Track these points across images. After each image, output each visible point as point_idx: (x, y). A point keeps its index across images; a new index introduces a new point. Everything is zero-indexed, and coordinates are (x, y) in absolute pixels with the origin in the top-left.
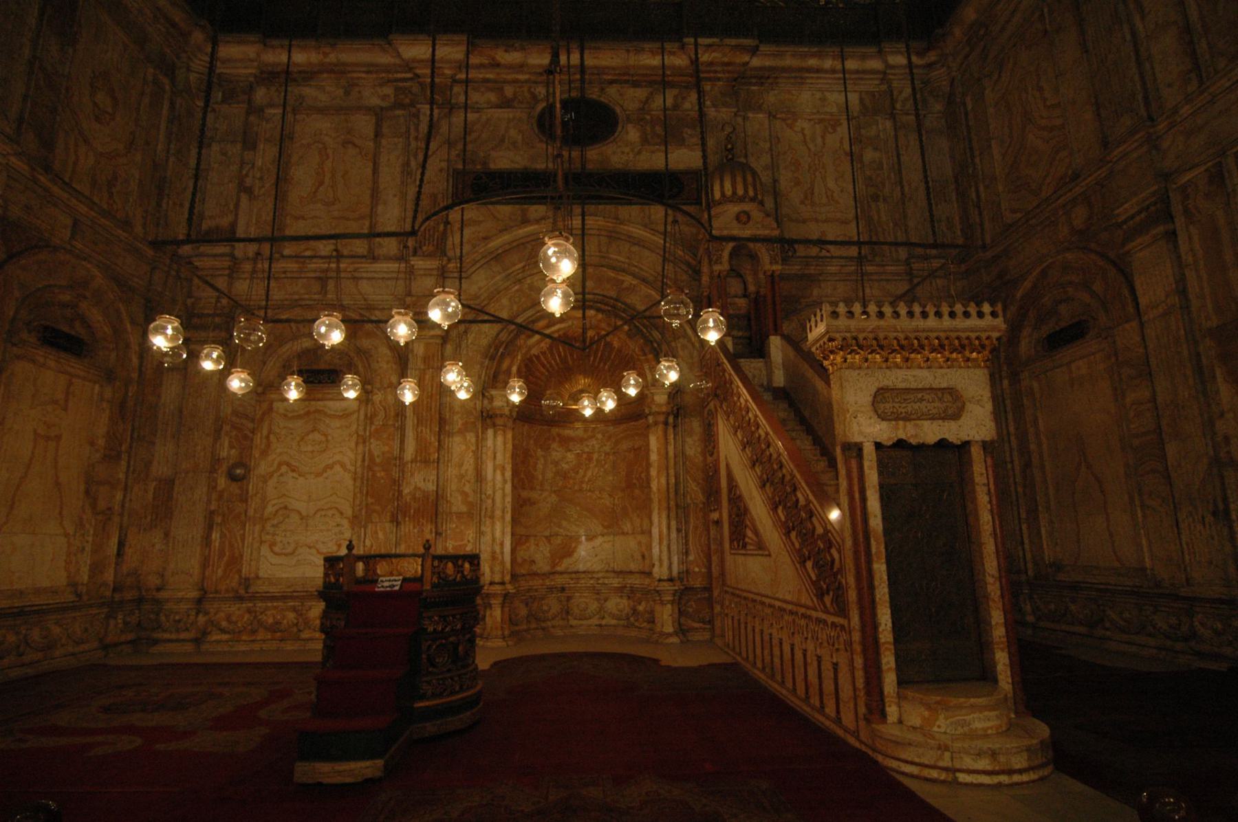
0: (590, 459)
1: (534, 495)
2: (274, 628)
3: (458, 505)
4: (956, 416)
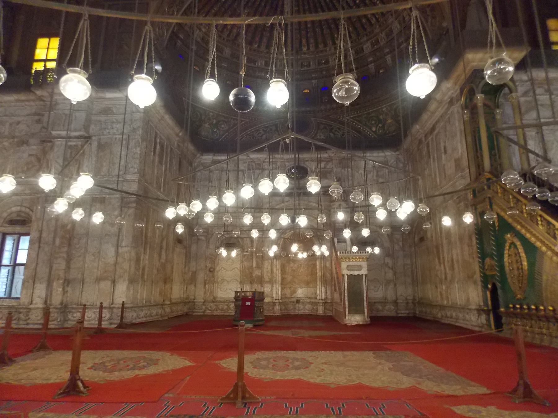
0: (301, 266)
1: (286, 276)
2: (222, 310)
3: (267, 279)
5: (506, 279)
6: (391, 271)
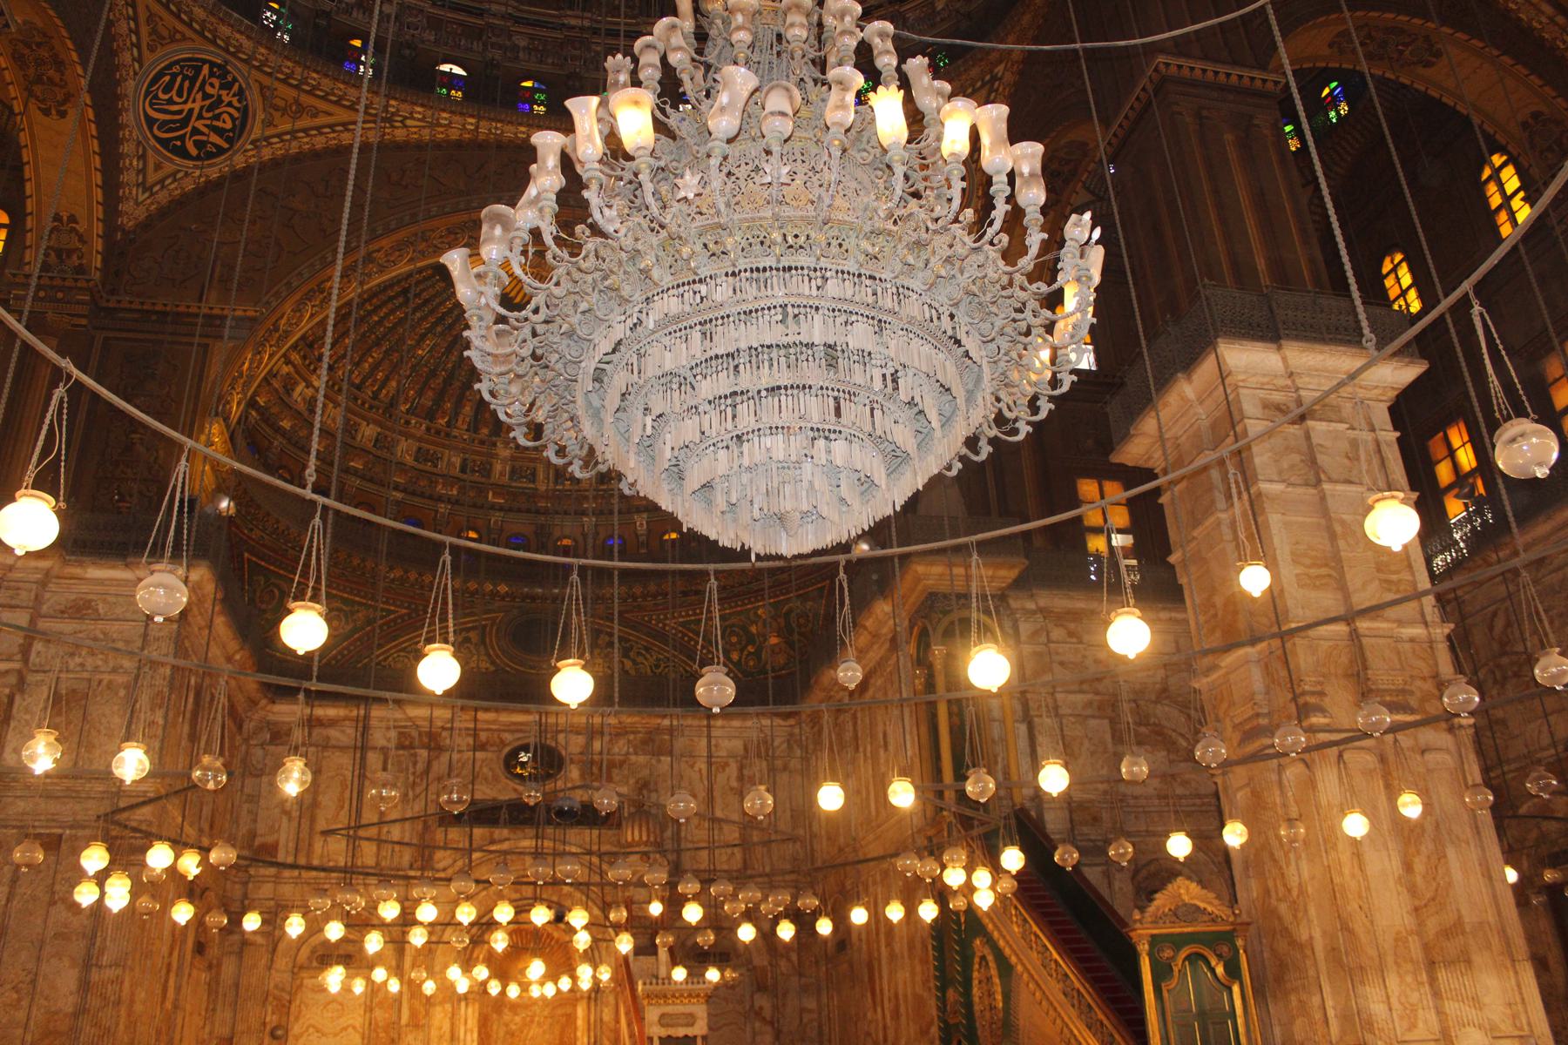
0: (532, 1022)
4: (692, 1025)
5: (975, 1029)
6: (769, 1028)
